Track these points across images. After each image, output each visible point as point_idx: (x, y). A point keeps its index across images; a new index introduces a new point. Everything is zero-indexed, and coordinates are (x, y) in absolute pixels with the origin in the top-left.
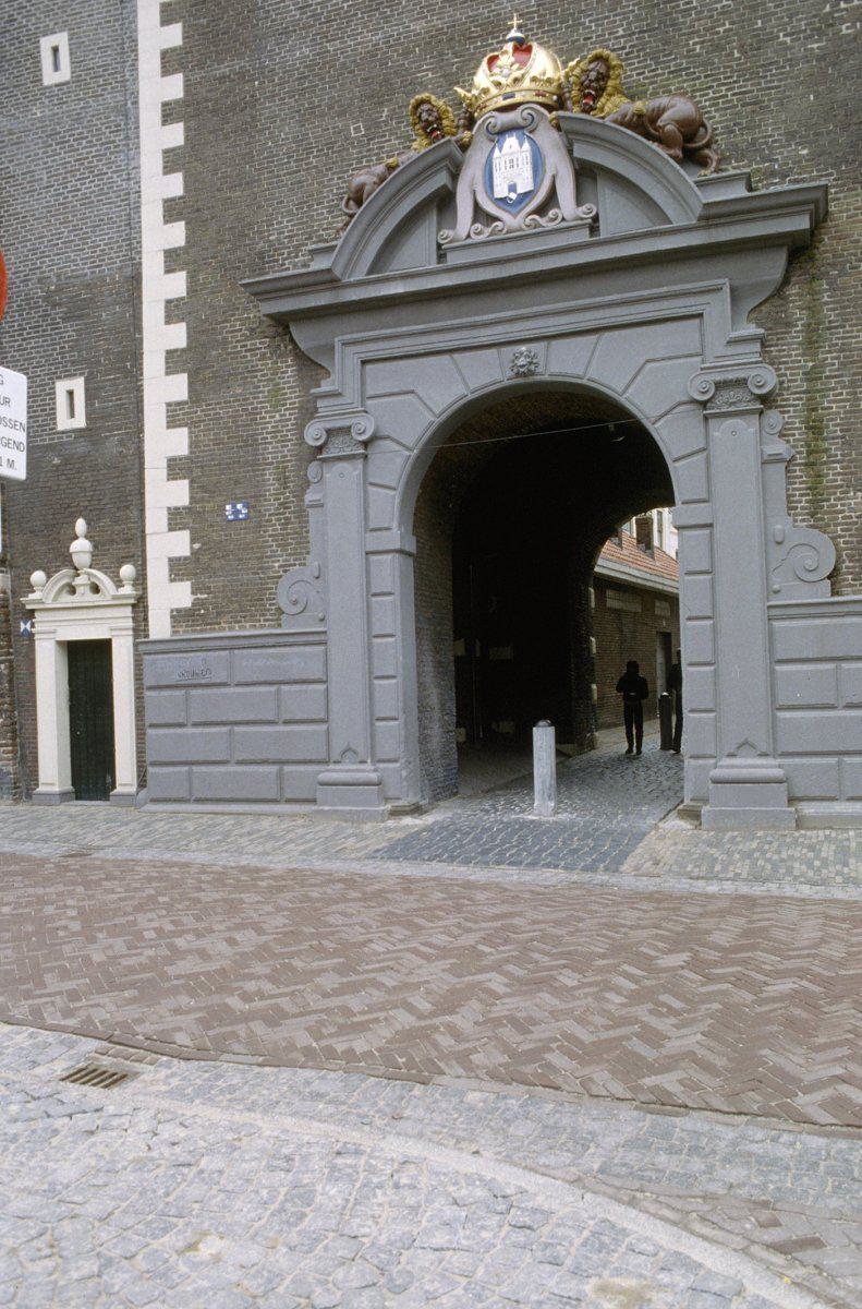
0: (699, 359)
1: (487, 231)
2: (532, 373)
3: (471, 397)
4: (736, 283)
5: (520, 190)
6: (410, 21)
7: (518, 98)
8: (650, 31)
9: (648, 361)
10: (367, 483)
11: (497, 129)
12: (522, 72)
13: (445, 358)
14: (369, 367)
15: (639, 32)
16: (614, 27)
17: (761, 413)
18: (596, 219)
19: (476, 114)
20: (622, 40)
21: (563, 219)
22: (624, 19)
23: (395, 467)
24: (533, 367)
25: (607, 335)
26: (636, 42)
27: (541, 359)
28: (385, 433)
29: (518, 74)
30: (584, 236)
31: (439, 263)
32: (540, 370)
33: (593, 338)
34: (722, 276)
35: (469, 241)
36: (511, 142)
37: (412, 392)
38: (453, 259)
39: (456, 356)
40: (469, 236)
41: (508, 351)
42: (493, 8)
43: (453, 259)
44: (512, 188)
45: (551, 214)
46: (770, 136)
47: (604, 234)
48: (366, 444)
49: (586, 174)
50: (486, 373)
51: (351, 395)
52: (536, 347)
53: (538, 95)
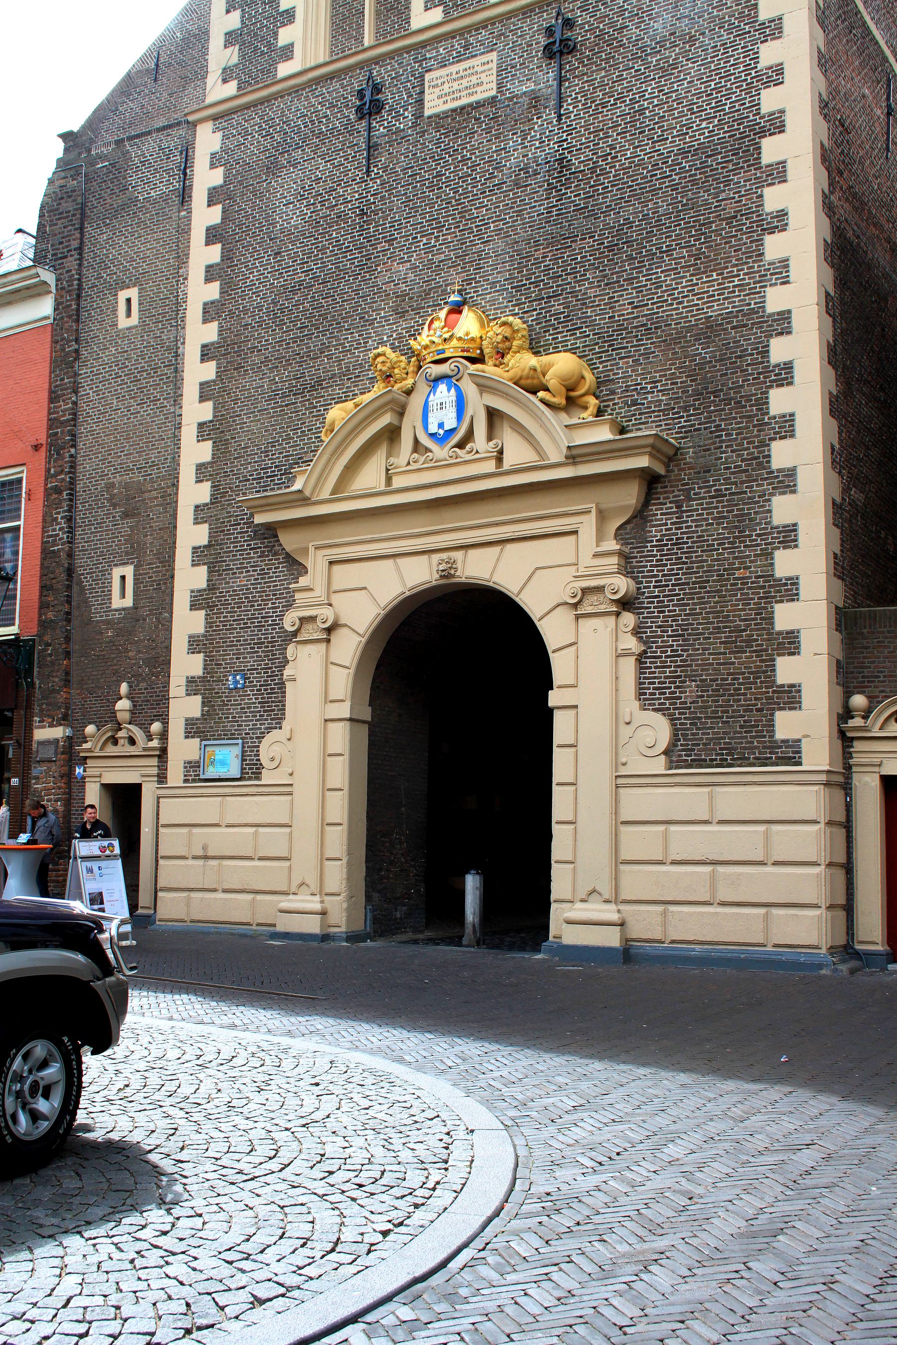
0: (574, 568)
2: (453, 576)
3: (408, 594)
4: (602, 506)
6: (383, 284)
9: (537, 569)
10: (328, 663)
13: (390, 562)
14: (336, 568)
17: (618, 614)
21: (477, 452)
22: (536, 287)
23: (348, 648)
24: (452, 572)
25: (509, 547)
27: (459, 565)
28: (342, 622)
32: (458, 574)
33: (496, 549)
34: (588, 501)
36: (442, 387)
37: (365, 588)
39: (401, 561)
40: (409, 464)
41: (436, 557)
45: (468, 447)
48: (329, 630)
50: (420, 574)
51: (319, 592)
52: (458, 555)
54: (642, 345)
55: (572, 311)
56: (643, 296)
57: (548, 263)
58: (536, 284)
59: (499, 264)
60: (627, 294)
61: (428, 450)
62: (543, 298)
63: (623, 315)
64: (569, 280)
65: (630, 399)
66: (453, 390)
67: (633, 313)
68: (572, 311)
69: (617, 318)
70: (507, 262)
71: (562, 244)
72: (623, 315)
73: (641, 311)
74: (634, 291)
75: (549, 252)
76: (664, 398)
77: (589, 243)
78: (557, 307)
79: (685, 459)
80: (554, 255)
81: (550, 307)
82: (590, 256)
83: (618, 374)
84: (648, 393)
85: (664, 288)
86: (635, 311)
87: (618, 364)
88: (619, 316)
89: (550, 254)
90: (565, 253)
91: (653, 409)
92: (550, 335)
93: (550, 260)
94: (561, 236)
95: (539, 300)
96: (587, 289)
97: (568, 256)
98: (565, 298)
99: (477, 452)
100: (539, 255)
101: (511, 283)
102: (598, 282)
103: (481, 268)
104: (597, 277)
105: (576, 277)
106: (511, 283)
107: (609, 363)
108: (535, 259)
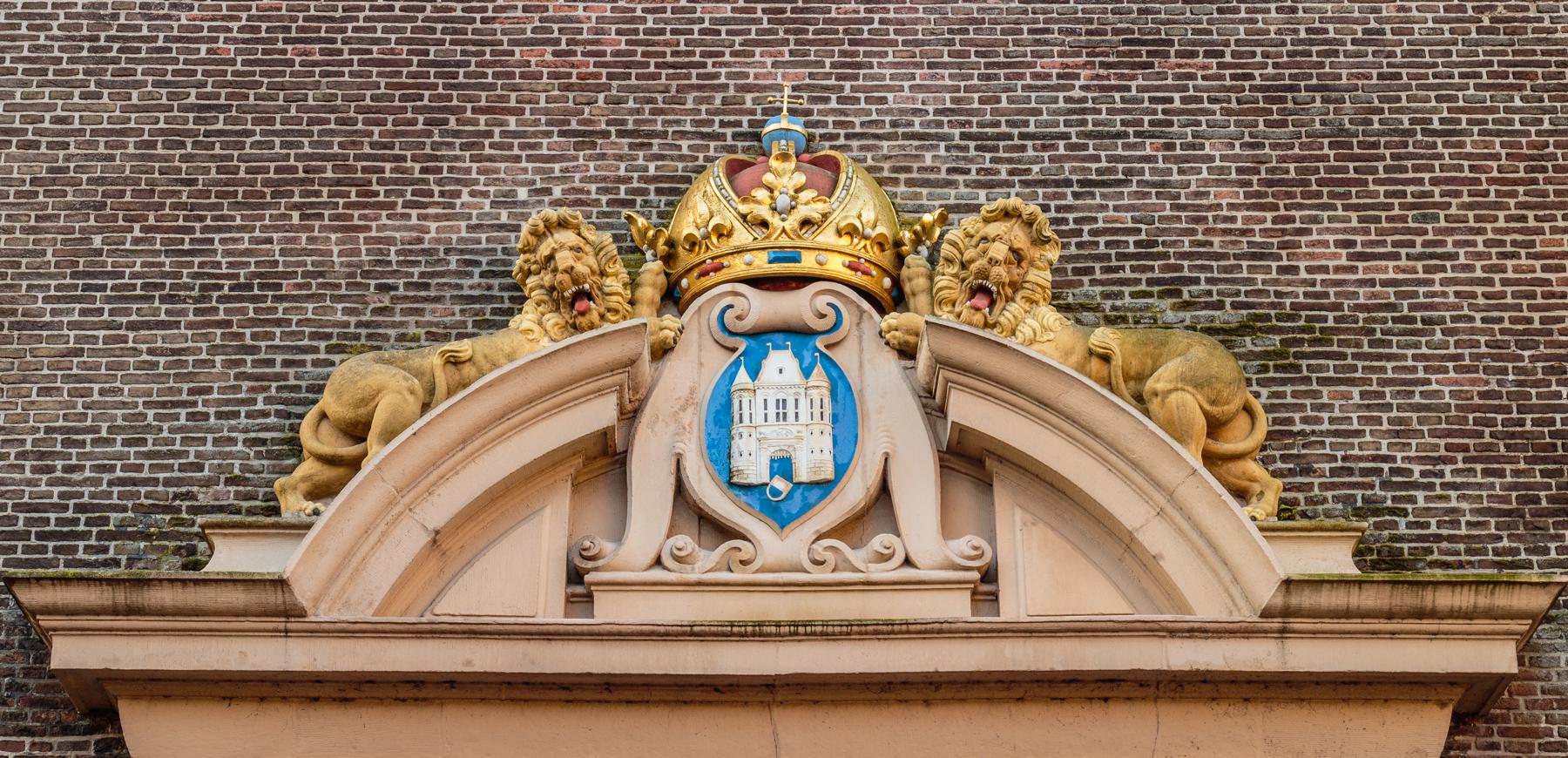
1: (707, 560)
5: (803, 474)
7: (808, 263)
8: (1103, 184)
11: (747, 324)
12: (821, 207)
15: (1082, 183)
16: (1019, 161)
18: (989, 575)
19: (684, 282)
20: (1040, 191)
22: (1044, 148)
26: (1070, 201)
29: (814, 211)
30: (957, 607)
31: (566, 616)
35: (657, 574)
38: (609, 610)
42: (727, 58)
43: (609, 610)
44: (782, 466)
46: (1385, 459)
47: (1012, 609)
49: (969, 462)
53: (851, 267)
54: (1389, 357)
55: (1163, 231)
56: (1380, 232)
57: (1077, 93)
58: (1046, 141)
59: (918, 65)
60: (1330, 219)
61: (717, 530)
62: (1068, 183)
63: (1325, 269)
64: (1148, 151)
65: (1359, 493)
66: (819, 377)
67: (1353, 269)
68: (1163, 231)
69: (1303, 275)
70: (945, 66)
71: (1119, 54)
72: (1325, 269)
73: (1378, 270)
74: (1354, 215)
75: (1085, 65)
76: (1465, 505)
77: (1205, 67)
78: (1110, 210)
79: (1548, 678)
80: (1098, 77)
81: (1090, 208)
82: (1212, 100)
83: (1319, 421)
84: (1415, 486)
85: (1443, 224)
86: (1360, 265)
87: (1316, 394)
88: (1309, 270)
89: (1084, 73)
90: (1134, 77)
91: (1433, 529)
92: (1093, 282)
93: (1084, 88)
94: (1116, 32)
95: (1057, 184)
96: (1206, 183)
97: (1140, 89)
98: (1137, 195)
99: (908, 562)
100: (1052, 65)
101: (962, 124)
102: (1239, 171)
103: (859, 66)
104: (1236, 158)
105: (1171, 147)
106: (962, 124)
107: (1289, 389)
108: (1036, 76)
